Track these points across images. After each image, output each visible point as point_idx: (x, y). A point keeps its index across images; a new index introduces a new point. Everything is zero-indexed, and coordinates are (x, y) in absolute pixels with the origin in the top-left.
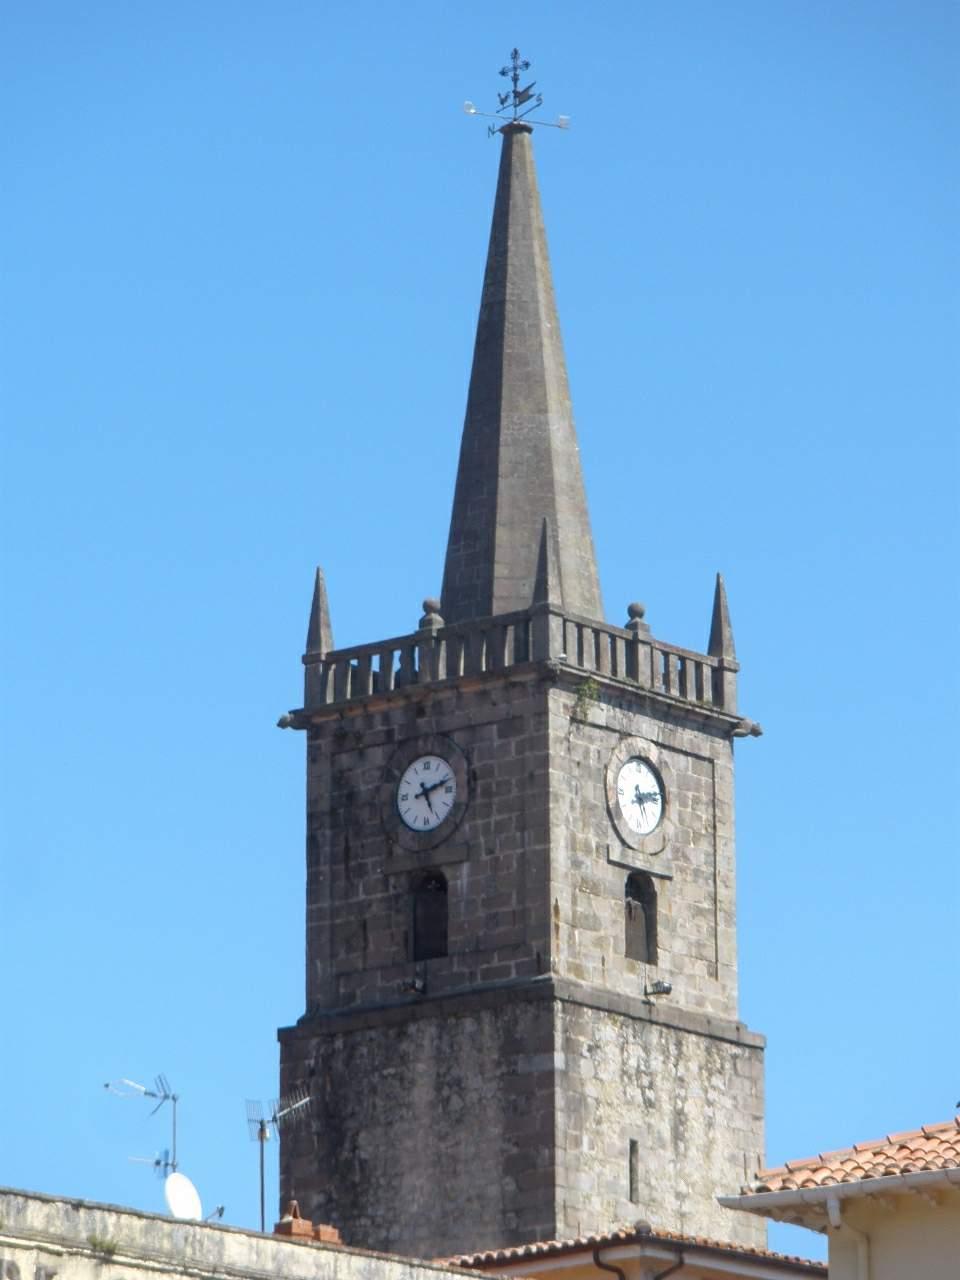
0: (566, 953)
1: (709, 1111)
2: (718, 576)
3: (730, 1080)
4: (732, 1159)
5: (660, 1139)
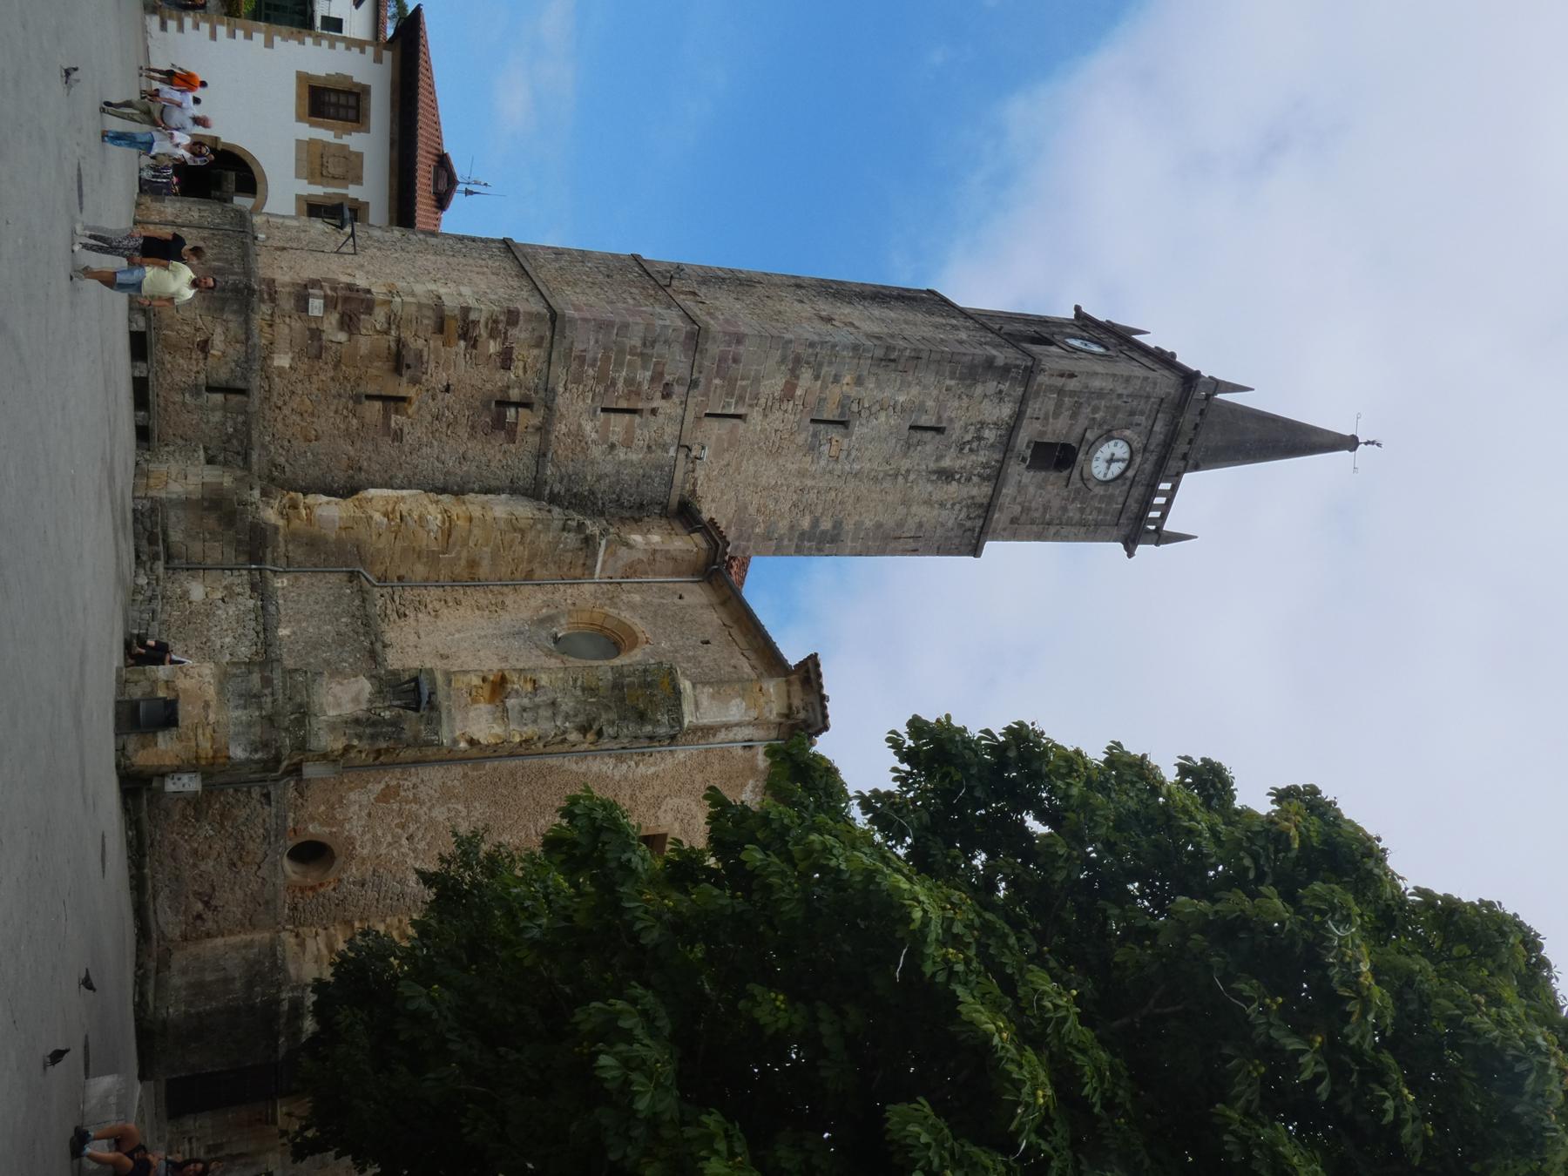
1: (949, 506)
3: (963, 525)
4: (920, 525)
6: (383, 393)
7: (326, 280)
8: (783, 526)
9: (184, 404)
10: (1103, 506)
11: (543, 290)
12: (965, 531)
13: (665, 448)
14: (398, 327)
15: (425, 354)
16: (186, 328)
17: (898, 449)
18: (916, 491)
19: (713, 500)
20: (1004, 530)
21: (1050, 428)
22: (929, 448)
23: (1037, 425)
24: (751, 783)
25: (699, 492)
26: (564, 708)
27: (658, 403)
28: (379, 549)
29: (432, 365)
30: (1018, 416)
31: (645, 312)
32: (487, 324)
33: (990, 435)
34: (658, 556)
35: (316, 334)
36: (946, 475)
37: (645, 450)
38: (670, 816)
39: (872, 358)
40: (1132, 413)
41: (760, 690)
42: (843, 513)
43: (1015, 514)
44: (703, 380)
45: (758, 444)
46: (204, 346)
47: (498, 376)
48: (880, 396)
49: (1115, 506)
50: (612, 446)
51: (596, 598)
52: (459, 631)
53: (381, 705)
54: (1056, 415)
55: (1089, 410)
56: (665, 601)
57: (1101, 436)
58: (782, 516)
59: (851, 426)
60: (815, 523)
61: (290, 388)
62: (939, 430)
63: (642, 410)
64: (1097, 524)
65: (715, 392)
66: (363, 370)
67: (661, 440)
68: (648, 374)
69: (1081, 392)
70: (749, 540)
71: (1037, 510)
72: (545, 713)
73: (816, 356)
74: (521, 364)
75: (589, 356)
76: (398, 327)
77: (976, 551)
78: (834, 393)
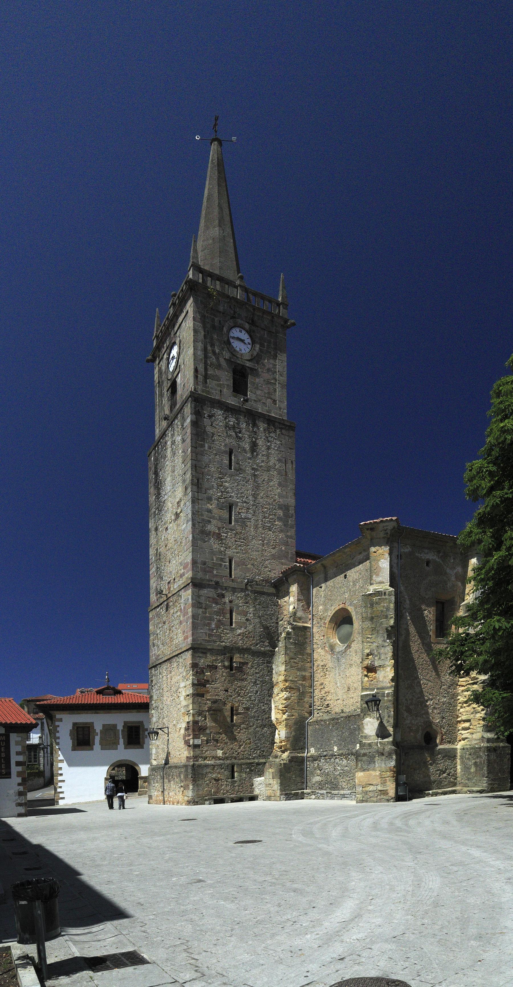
7: (184, 738)
31: (184, 608)
33: (232, 421)
36: (254, 446)
39: (198, 492)
44: (215, 579)
46: (217, 780)
54: (218, 379)
63: (230, 607)
73: (199, 522)
78: (216, 512)
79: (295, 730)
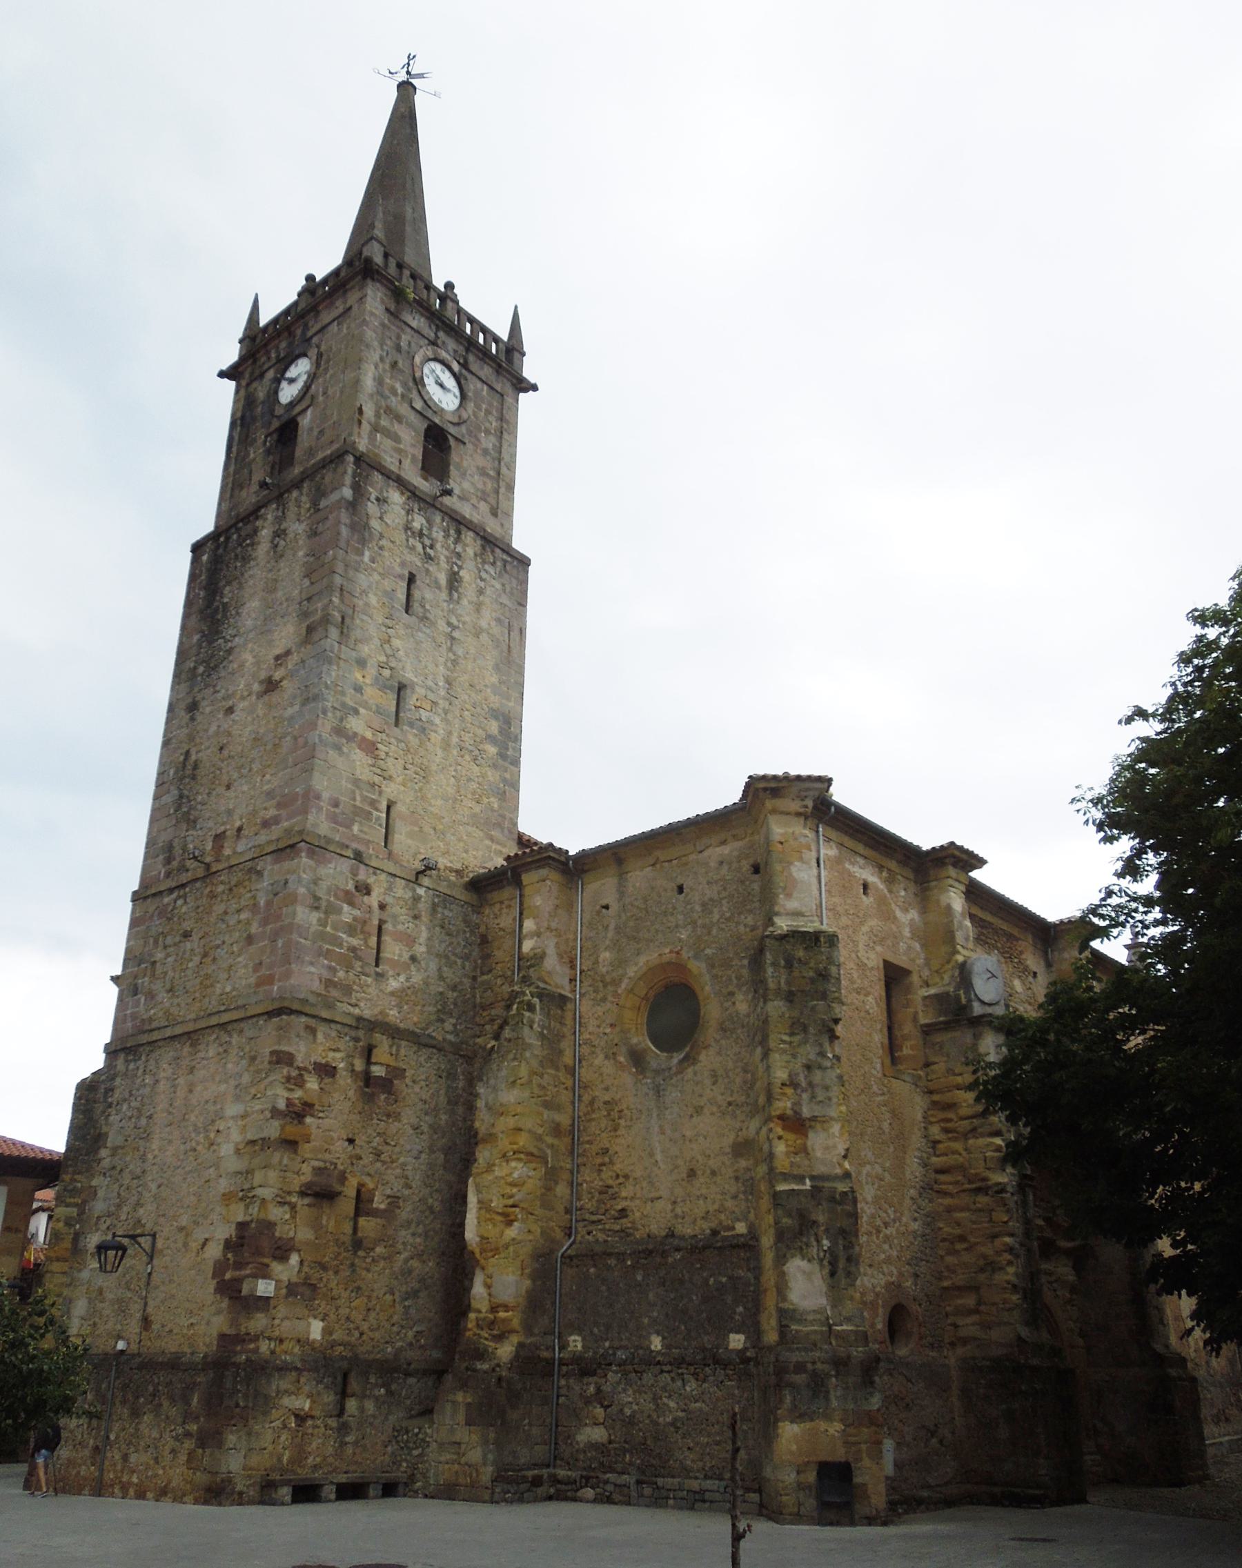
0: (366, 441)
1: (482, 584)
2: (516, 307)
3: (500, 572)
4: (498, 620)
5: (436, 581)
6: (352, 1215)
8: (492, 776)
9: (356, 1443)
10: (484, 406)
11: (225, 1018)
12: (506, 571)
13: (416, 899)
14: (289, 1193)
15: (316, 1164)
16: (283, 1438)
17: (428, 631)
18: (467, 619)
19: (466, 852)
20: (502, 525)
21: (411, 450)
22: (428, 595)
23: (407, 463)
24: (847, 866)
25: (458, 866)
26: (812, 1056)
27: (374, 900)
28: (542, 1233)
29: (327, 1156)
30: (402, 484)
31: (269, 904)
32: (291, 1090)
33: (418, 522)
34: (554, 925)
35: (291, 1290)
36: (454, 581)
37: (417, 922)
38: (872, 956)
39: (340, 643)
40: (398, 348)
41: (781, 843)
42: (485, 707)
43: (488, 510)
44: (354, 845)
45: (416, 791)
46: (301, 1418)
47: (342, 1082)
48: (376, 642)
49: (485, 393)
50: (413, 959)
51: (604, 1000)
52: (651, 1155)
53: (815, 1250)
54: (397, 439)
55: (393, 399)
56: (612, 926)
57: (420, 392)
58: (483, 776)
59: (405, 682)
60: (490, 738)
61: (343, 1321)
62: (411, 579)
64: (501, 419)
65: (366, 833)
66: (330, 1237)
67: (409, 902)
68: (346, 907)
69: (376, 404)
70: (503, 817)
71: (484, 483)
72: (817, 1076)
73: (335, 708)
74: (331, 1054)
75: (326, 974)
76: (289, 1193)
77: (524, 562)
78: (371, 694)
79: (534, 1277)
